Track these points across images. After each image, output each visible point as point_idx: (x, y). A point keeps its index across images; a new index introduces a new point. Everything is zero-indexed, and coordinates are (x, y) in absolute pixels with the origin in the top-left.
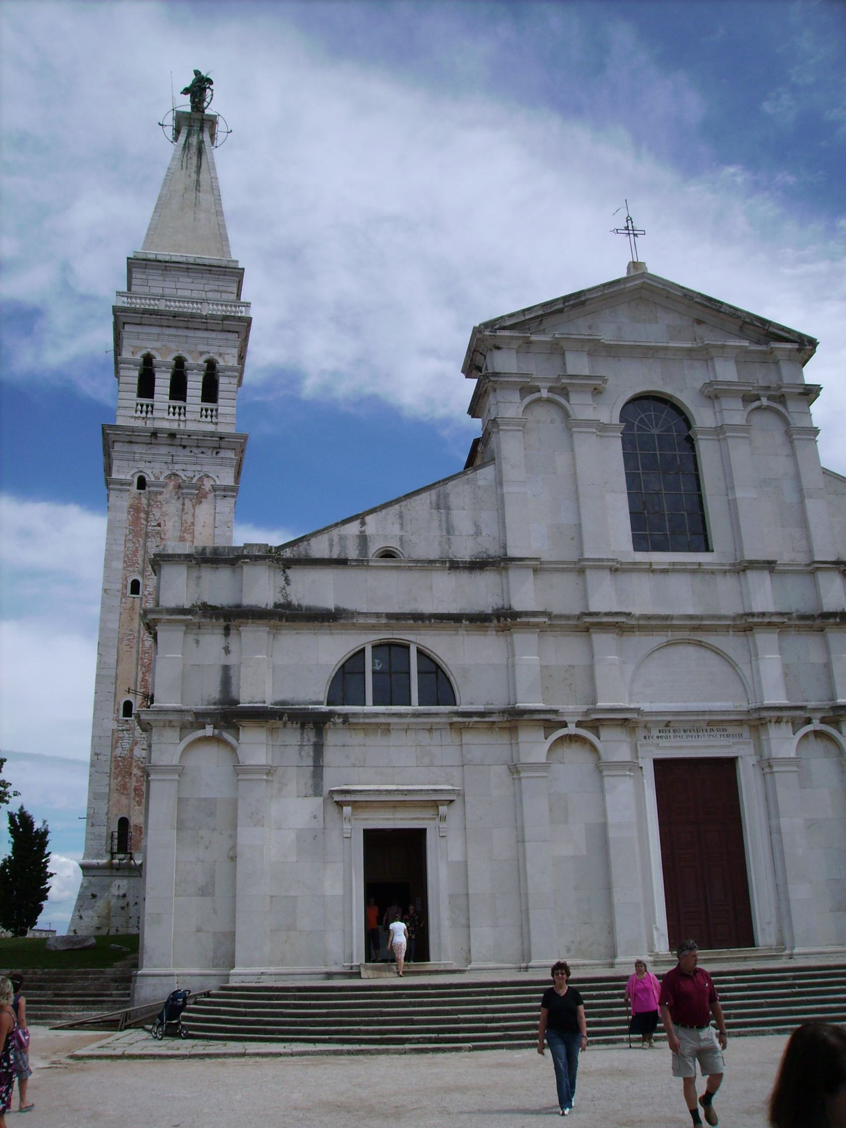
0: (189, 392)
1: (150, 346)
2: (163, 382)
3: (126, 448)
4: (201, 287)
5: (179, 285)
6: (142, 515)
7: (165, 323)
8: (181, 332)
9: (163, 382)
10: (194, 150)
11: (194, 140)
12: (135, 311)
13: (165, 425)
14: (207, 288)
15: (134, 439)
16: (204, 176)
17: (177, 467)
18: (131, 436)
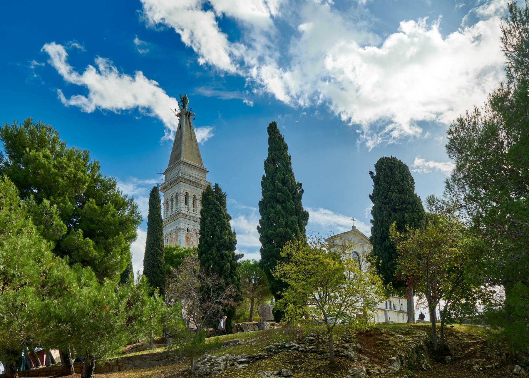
0: (197, 206)
1: (188, 190)
2: (190, 201)
3: (184, 219)
4: (198, 174)
5: (193, 172)
6: (189, 240)
7: (191, 184)
8: (195, 188)
9: (190, 201)
10: (188, 125)
11: (188, 121)
12: (185, 179)
13: (192, 215)
14: (200, 175)
15: (186, 218)
16: (192, 135)
17: (196, 227)
18: (186, 216)
